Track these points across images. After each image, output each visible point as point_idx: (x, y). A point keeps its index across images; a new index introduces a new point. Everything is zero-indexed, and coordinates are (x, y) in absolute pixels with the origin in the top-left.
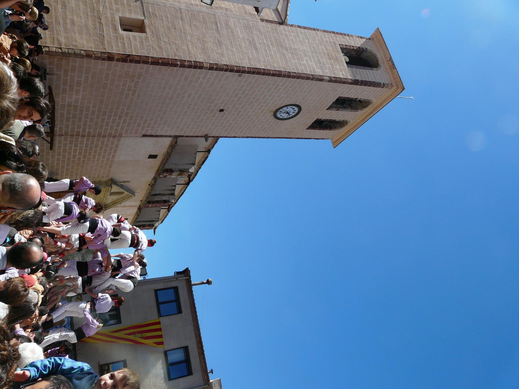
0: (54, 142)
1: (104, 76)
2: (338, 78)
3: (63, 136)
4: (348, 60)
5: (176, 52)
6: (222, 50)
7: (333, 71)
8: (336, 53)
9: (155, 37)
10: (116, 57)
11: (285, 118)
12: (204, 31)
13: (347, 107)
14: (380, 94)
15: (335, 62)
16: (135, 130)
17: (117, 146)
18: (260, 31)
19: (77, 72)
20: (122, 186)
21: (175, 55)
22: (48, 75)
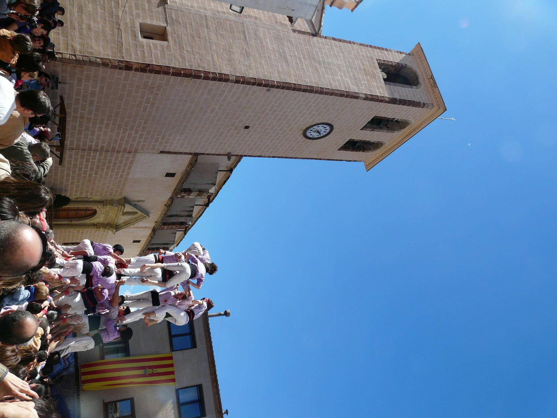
0: (63, 156)
1: (120, 87)
2: (375, 95)
3: (74, 149)
4: (386, 77)
5: (200, 62)
6: (249, 62)
7: (369, 88)
8: (373, 68)
9: (178, 46)
10: (134, 67)
12: (231, 41)
13: (383, 127)
14: (420, 114)
15: (371, 78)
16: (152, 146)
17: (132, 162)
18: (291, 42)
19: (91, 81)
20: (135, 206)
21: (199, 66)
22: (60, 84)
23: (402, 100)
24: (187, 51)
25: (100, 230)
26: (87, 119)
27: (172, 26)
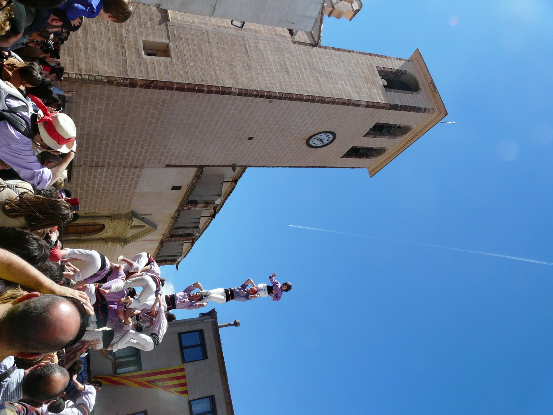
0: (72, 173)
1: (126, 104)
2: (376, 103)
3: (82, 166)
4: (386, 84)
6: (251, 74)
7: (370, 95)
10: (139, 83)
11: (318, 145)
12: (233, 54)
13: (385, 133)
15: (372, 86)
16: (157, 160)
17: (138, 177)
18: (291, 53)
19: (97, 99)
20: (143, 220)
21: (202, 80)
22: (67, 103)
23: (403, 106)
24: (190, 66)
25: (109, 244)
26: (93, 136)
27: (174, 42)
